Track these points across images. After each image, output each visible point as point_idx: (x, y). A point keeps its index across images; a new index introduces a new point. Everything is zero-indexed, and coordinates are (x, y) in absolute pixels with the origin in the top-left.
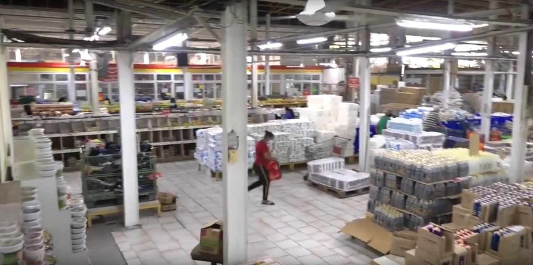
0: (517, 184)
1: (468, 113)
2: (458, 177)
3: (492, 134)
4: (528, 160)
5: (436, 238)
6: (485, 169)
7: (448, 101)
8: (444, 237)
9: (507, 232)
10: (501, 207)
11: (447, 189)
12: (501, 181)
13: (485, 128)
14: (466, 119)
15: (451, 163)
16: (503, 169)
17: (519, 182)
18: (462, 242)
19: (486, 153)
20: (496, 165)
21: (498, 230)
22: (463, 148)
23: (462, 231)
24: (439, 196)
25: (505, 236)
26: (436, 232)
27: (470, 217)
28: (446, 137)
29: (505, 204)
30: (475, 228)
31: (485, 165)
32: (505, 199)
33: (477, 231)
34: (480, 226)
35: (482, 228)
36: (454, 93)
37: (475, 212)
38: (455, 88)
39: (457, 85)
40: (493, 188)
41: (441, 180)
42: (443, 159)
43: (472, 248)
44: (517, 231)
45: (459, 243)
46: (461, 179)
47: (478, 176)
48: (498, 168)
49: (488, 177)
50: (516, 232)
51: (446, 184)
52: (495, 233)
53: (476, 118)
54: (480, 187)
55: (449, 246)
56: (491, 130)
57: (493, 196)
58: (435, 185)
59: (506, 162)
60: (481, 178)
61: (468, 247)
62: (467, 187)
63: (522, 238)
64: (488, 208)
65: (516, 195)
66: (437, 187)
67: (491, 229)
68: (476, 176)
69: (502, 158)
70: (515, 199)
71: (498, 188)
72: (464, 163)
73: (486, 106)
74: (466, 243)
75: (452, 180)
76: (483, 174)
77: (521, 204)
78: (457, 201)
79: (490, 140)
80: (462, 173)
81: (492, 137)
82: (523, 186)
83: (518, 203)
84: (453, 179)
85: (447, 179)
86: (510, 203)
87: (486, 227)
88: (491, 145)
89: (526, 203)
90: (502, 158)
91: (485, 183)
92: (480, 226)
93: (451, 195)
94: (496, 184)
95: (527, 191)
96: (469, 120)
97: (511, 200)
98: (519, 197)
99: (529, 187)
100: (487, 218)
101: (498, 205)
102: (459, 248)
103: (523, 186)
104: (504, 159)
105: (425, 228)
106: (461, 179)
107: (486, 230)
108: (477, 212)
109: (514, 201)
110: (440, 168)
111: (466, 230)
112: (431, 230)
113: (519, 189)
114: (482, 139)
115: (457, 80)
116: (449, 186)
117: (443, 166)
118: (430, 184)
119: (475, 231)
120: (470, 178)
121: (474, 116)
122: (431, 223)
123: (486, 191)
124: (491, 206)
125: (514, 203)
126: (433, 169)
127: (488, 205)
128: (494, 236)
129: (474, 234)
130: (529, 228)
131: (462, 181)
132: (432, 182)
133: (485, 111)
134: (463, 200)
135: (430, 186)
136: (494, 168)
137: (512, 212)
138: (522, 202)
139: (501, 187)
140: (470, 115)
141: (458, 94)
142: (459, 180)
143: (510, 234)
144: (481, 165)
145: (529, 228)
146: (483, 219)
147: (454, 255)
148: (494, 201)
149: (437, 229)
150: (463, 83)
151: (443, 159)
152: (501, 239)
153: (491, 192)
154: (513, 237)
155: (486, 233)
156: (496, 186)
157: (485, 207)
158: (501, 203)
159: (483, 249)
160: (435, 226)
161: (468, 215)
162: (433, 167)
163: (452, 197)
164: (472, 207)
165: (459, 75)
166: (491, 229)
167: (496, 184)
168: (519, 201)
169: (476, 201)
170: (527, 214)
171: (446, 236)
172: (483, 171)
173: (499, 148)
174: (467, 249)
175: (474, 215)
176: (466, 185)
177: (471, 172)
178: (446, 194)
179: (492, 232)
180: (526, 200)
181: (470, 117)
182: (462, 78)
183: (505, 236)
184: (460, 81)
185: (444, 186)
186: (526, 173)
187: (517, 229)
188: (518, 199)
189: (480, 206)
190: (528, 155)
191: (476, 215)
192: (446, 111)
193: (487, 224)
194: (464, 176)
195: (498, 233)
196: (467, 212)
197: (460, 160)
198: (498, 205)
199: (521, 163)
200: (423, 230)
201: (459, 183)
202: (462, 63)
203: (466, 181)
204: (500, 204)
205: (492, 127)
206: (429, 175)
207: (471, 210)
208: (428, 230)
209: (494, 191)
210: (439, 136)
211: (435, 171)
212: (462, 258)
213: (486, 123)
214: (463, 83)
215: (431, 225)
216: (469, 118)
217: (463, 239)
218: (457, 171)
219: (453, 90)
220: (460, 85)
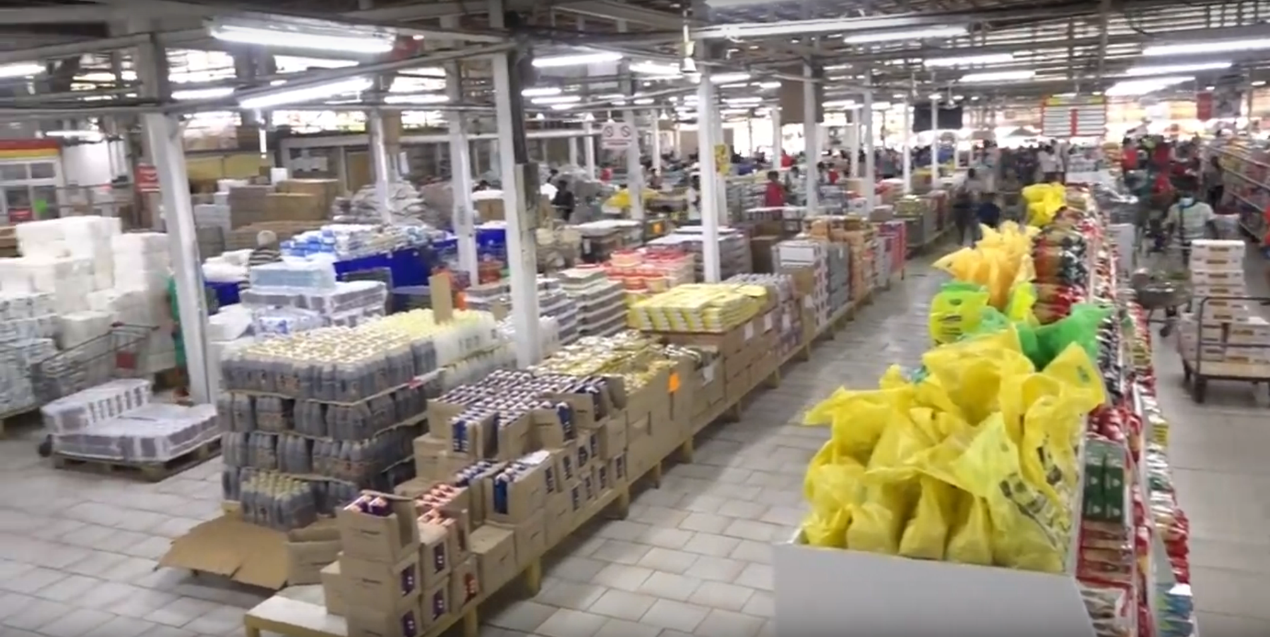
0: (531, 368)
1: (433, 228)
2: (417, 374)
3: (483, 269)
4: (548, 314)
5: (377, 522)
6: (468, 346)
7: (389, 206)
8: (393, 516)
9: (521, 469)
10: (502, 422)
11: (397, 405)
12: (505, 367)
13: (468, 258)
14: (430, 241)
15: (397, 348)
16: (503, 343)
17: (534, 363)
18: (438, 515)
19: (468, 314)
20: (488, 335)
21: (502, 471)
22: (423, 308)
23: (436, 492)
24: (381, 426)
25: (517, 479)
26: (377, 511)
27: (450, 458)
28: (388, 288)
29: (512, 414)
30: (460, 477)
31: (468, 340)
32: (510, 402)
33: (465, 483)
34: (468, 471)
35: (473, 475)
36: (400, 186)
37: (457, 444)
38: (401, 174)
39: (405, 169)
40: (486, 385)
41: (381, 389)
42: (380, 342)
43: (456, 523)
44: (537, 462)
45: (431, 518)
46: (423, 378)
47: (459, 365)
48: (495, 341)
49: (476, 364)
50: (535, 465)
51: (393, 395)
52: (498, 477)
53: (450, 237)
54: (462, 387)
55: (407, 532)
56: (480, 259)
57: (487, 403)
58: (369, 403)
59: (507, 328)
60: (464, 367)
61: (448, 522)
62: (437, 393)
63: (548, 473)
64: (480, 429)
65: (529, 392)
66: (375, 406)
67: (490, 471)
68: (454, 366)
69: (499, 317)
70: (527, 399)
71: (497, 384)
72: (424, 341)
73: (462, 211)
74: (444, 514)
75: (404, 385)
76: (466, 359)
77: (537, 408)
78: (421, 428)
79: (481, 282)
80: (424, 365)
81: (483, 276)
82: (541, 370)
83: (533, 406)
84: (406, 382)
85: (391, 386)
86: (519, 409)
87: (480, 471)
88: (479, 294)
89: (546, 403)
90: (499, 317)
91: (474, 378)
92: (468, 471)
93: (407, 417)
94: (492, 375)
95: (548, 379)
96: (436, 245)
97: (521, 404)
98: (534, 394)
99: (551, 369)
100: (480, 452)
101: (497, 418)
102: (430, 530)
103: (541, 370)
104: (506, 319)
105: (353, 506)
106: (423, 378)
107: (481, 475)
108: (460, 442)
109: (526, 404)
110: (376, 363)
111: (443, 487)
112: (364, 507)
113: (535, 378)
114: (461, 283)
115: (403, 155)
116: (400, 397)
117: (382, 357)
118: (358, 402)
119: (458, 485)
120: (441, 373)
121: (445, 235)
122: (364, 492)
123: (473, 393)
124: (485, 423)
125: (526, 408)
126: (359, 369)
127: (478, 424)
128: (497, 483)
129: (458, 491)
130: (558, 451)
131: (428, 383)
132: (363, 397)
133: (462, 222)
134: (432, 424)
135: (358, 408)
136: (488, 342)
137: (524, 429)
138: (541, 402)
139: (501, 380)
140: (436, 233)
141: (410, 188)
142: (419, 381)
143: (526, 473)
144: (460, 343)
145: (558, 451)
146: (474, 452)
147: (422, 548)
148: (489, 413)
149: (378, 501)
150: (418, 162)
151: (380, 342)
152: (510, 486)
153: (481, 394)
154: (533, 475)
155: (482, 484)
156: (491, 380)
157: (474, 428)
158: (503, 414)
159: (478, 518)
160: (373, 497)
161: (444, 453)
162: (360, 364)
163: (411, 421)
164: (450, 433)
165: (405, 146)
166: (490, 471)
167: (492, 375)
168: (535, 403)
169: (455, 420)
170: (550, 424)
171: (397, 513)
172: (466, 352)
173: (494, 297)
174: (448, 527)
175: (456, 451)
176: (436, 389)
177: (442, 358)
178: (398, 418)
179: (493, 476)
180: (547, 396)
181: (438, 237)
182: (416, 152)
183: (517, 479)
184: (409, 158)
185: (390, 401)
186: (546, 343)
187: (538, 458)
188: (533, 397)
189: (464, 429)
190: (544, 304)
191: (460, 449)
192: (386, 229)
193: (481, 463)
194: (428, 371)
195: (502, 475)
196: (442, 447)
197: (418, 338)
198: (497, 418)
199: (533, 325)
200: (349, 511)
201: (420, 388)
202: (411, 119)
203: (434, 381)
204: (501, 416)
205: (480, 253)
206: (353, 383)
207: (449, 441)
208: (359, 509)
209: (490, 390)
210: (371, 291)
211: (365, 373)
212: (438, 550)
213: (468, 247)
214: (418, 162)
215: (365, 496)
216: (436, 240)
217: (437, 509)
218: (411, 363)
219: (400, 179)
220: (413, 167)
